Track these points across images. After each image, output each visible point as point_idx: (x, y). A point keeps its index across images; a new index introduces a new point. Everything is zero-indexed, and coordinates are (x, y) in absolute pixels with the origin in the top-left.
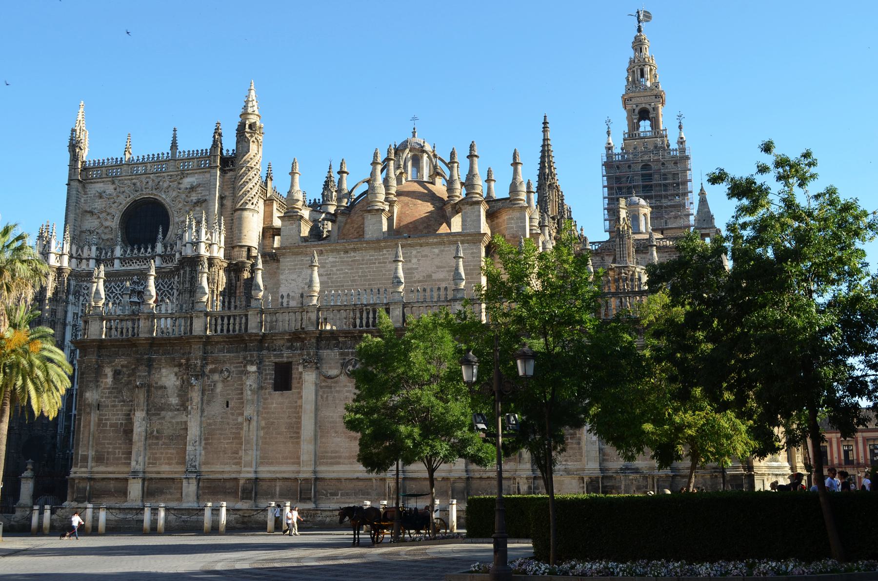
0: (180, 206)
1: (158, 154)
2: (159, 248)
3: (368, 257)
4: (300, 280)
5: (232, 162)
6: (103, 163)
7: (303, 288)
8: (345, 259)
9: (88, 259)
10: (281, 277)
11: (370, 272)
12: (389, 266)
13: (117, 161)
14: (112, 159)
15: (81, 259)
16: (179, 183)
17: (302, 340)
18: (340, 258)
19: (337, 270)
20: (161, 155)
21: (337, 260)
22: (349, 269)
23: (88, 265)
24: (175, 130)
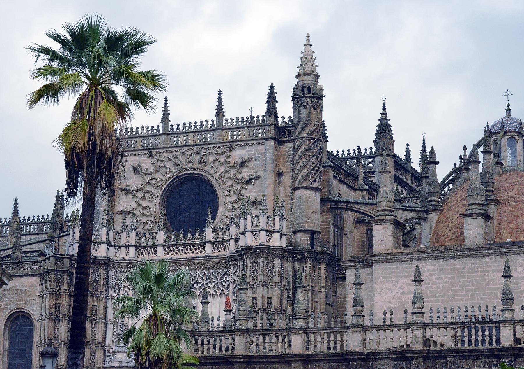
0: (230, 183)
1: (202, 122)
2: (209, 234)
3: (470, 265)
4: (397, 290)
5: (289, 131)
6: (137, 132)
7: (400, 298)
8: (445, 267)
9: (127, 247)
10: (375, 286)
11: (472, 281)
12: (492, 275)
13: (153, 130)
14: (148, 127)
15: (120, 247)
16: (229, 157)
17: (408, 359)
18: (439, 265)
19: (436, 279)
20: (204, 123)
21: (436, 268)
22: (449, 278)
23: (127, 253)
24: (220, 93)
